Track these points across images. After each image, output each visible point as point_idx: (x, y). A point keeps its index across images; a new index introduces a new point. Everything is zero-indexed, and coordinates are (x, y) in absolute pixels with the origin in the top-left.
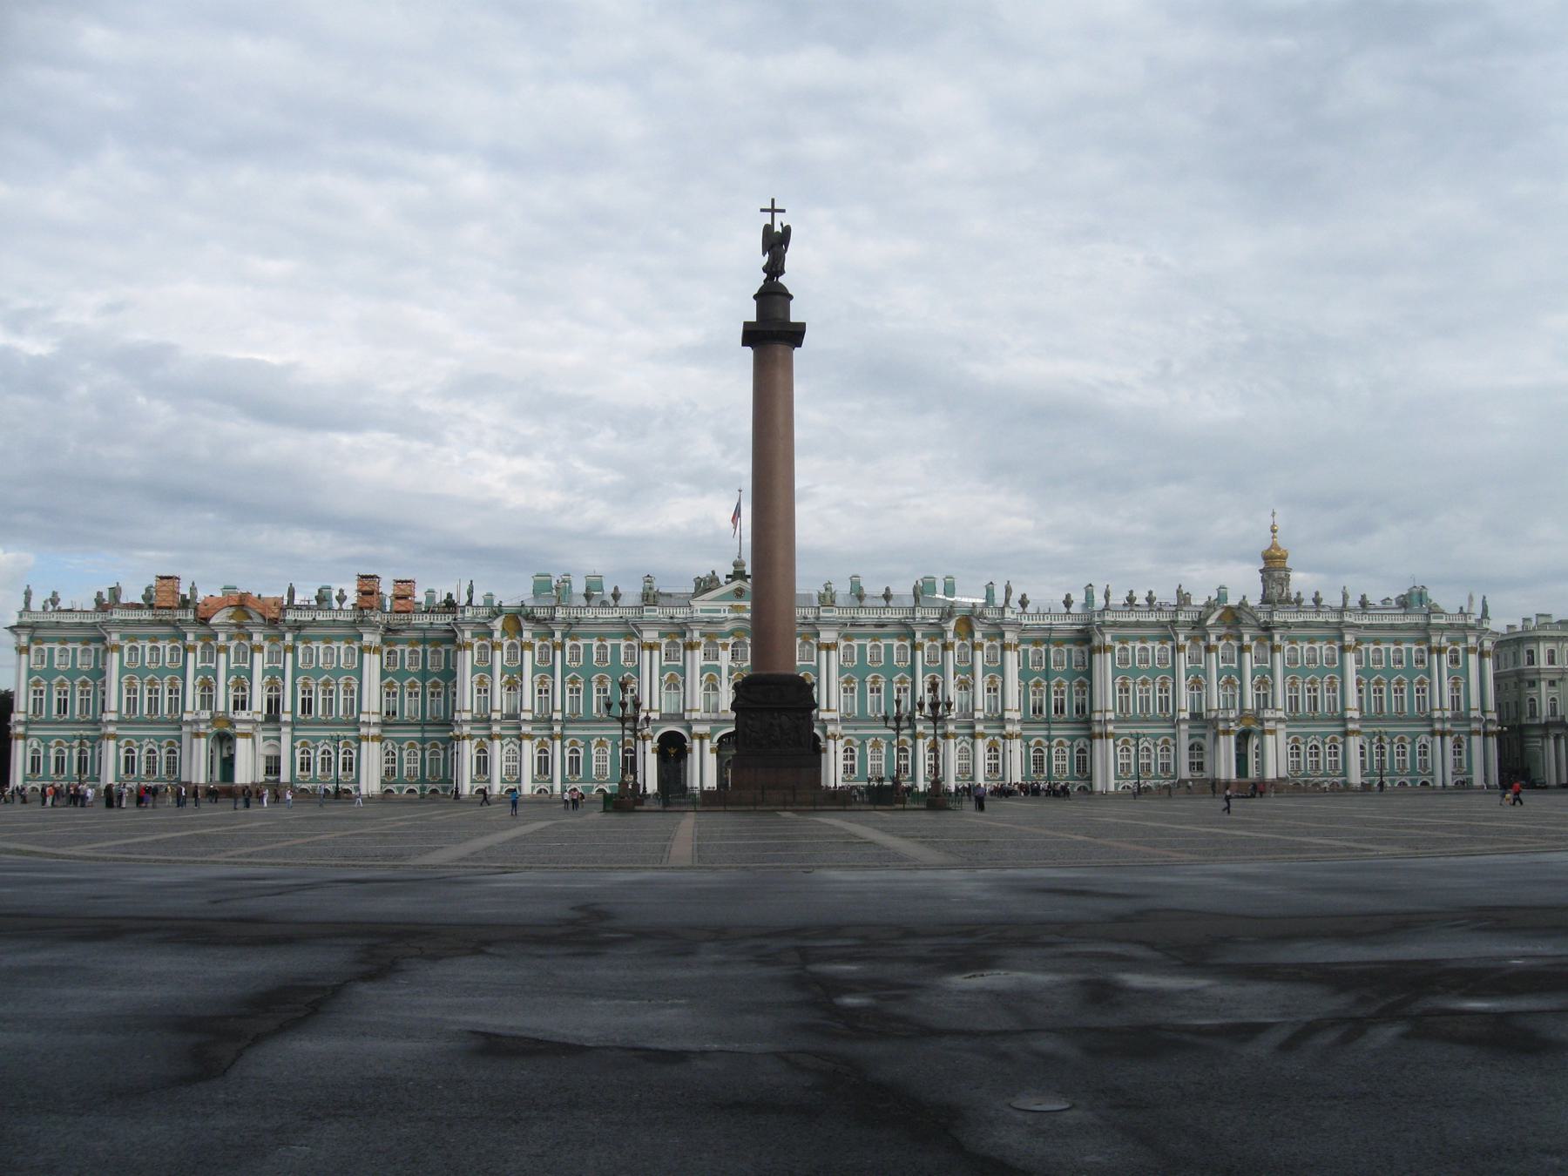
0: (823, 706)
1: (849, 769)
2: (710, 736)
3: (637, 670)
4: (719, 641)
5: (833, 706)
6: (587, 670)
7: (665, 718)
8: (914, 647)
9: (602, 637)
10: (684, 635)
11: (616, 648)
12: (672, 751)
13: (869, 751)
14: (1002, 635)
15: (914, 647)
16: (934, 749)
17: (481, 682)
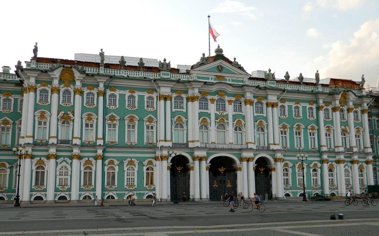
0: (271, 141)
1: (286, 182)
2: (206, 158)
3: (155, 113)
4: (209, 97)
5: (277, 142)
6: (121, 111)
7: (176, 146)
8: (318, 108)
9: (132, 90)
10: (186, 92)
11: (141, 98)
12: (179, 169)
13: (297, 171)
14: (360, 105)
15: (318, 108)
16: (330, 170)
17: (42, 116)
